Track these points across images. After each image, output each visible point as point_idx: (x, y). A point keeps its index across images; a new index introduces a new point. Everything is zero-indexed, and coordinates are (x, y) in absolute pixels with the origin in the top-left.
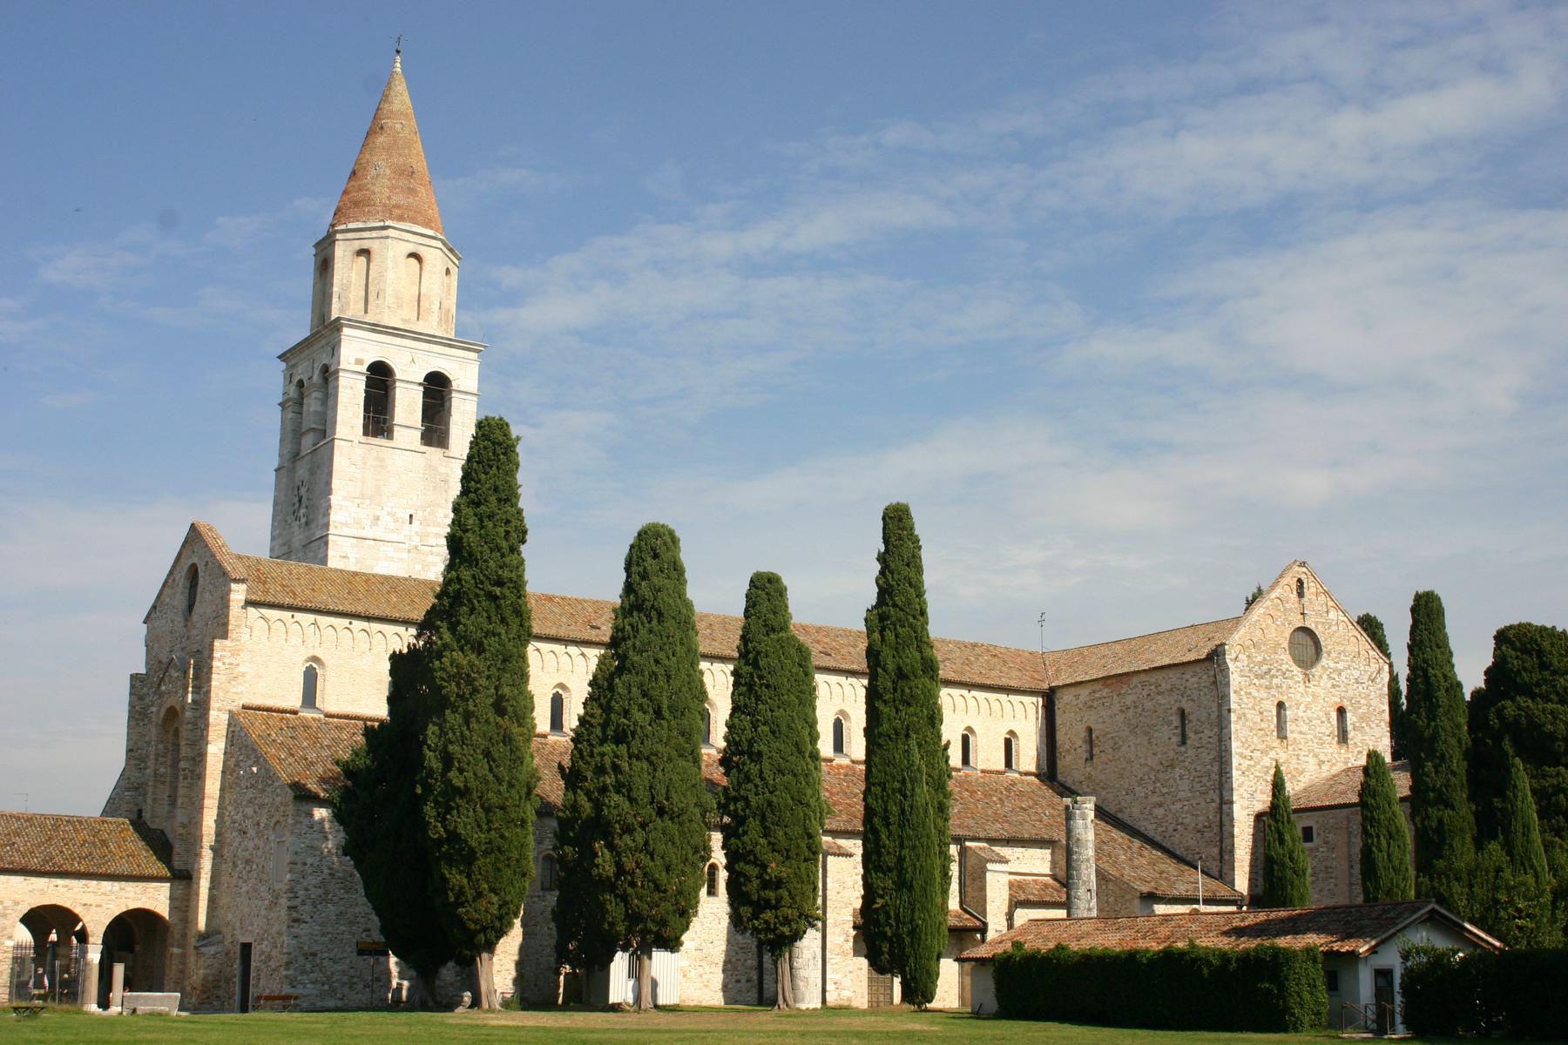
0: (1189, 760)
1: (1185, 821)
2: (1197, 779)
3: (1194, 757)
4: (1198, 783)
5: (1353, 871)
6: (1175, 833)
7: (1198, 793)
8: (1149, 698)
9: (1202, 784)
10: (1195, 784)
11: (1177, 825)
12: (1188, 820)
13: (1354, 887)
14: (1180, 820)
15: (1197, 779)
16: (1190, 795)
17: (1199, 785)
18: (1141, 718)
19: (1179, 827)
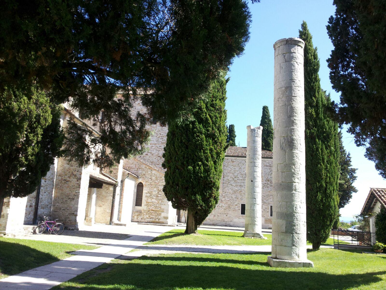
0: (157, 130)
1: (152, 152)
2: (161, 138)
3: (160, 129)
4: (161, 139)
5: (224, 179)
6: (146, 156)
7: (160, 143)
8: (139, 105)
9: (163, 140)
10: (159, 139)
11: (148, 153)
12: (154, 152)
13: (224, 184)
14: (150, 151)
15: (161, 138)
16: (156, 143)
17: (162, 140)
18: (134, 112)
19: (149, 154)
